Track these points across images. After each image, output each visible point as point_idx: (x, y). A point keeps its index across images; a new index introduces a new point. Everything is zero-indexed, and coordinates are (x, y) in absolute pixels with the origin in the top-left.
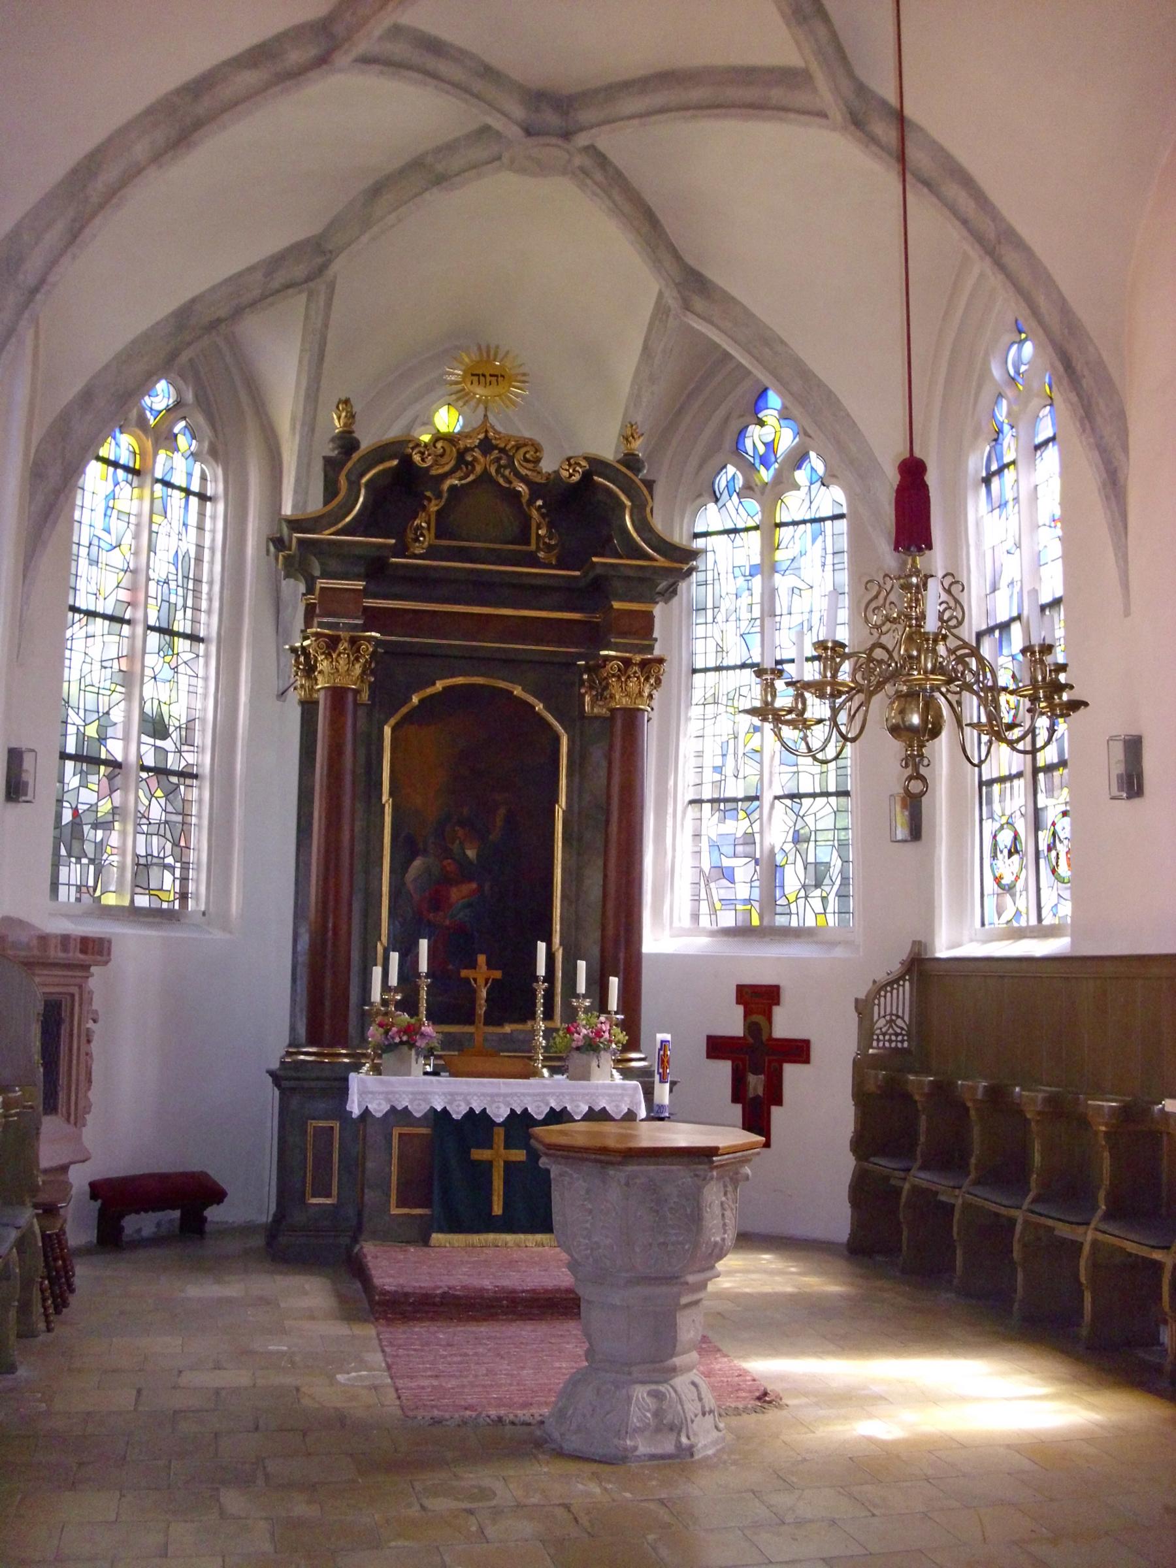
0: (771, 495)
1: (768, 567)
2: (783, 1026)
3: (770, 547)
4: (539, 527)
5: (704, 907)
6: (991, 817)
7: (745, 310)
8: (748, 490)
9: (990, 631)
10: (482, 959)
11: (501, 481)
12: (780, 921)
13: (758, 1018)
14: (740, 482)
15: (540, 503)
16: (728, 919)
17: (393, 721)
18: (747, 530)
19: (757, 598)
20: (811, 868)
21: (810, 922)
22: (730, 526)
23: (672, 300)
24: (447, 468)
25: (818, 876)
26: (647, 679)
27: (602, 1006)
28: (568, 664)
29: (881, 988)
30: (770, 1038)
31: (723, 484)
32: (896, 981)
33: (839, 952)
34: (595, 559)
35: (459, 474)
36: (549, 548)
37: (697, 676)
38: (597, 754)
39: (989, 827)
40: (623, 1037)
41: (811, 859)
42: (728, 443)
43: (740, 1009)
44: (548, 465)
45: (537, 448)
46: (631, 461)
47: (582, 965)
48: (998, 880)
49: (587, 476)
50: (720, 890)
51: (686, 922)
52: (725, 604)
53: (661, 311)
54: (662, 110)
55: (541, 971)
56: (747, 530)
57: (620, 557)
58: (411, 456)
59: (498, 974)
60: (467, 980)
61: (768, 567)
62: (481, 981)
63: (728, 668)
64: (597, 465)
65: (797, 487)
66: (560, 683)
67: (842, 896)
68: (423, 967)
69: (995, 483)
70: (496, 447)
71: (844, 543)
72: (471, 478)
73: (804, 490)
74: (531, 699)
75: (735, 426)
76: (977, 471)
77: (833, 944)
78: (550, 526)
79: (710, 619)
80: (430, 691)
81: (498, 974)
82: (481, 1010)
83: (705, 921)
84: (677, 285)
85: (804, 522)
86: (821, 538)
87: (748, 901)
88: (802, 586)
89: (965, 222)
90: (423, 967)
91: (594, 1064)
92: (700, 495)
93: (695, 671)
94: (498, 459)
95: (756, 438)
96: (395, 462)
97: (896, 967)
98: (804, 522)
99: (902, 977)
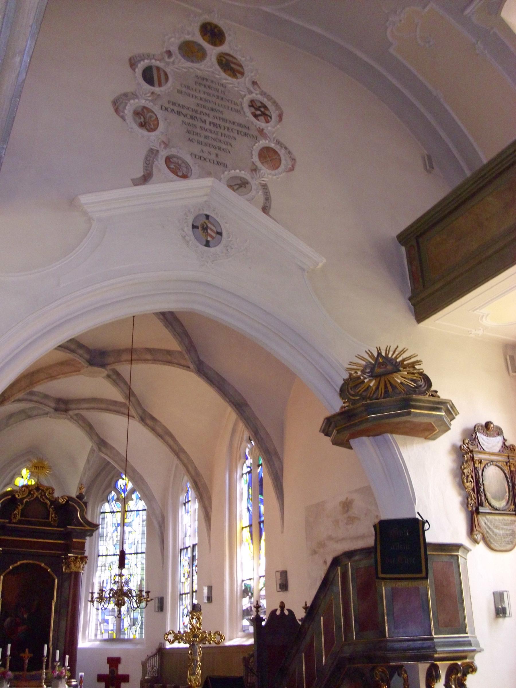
0: (125, 501)
1: (123, 524)
2: (122, 670)
3: (123, 518)
4: (52, 514)
5: (99, 632)
6: (182, 604)
7: (117, 451)
8: (118, 500)
9: (184, 549)
10: (27, 650)
11: (42, 500)
12: (122, 637)
13: (114, 669)
14: (116, 497)
15: (53, 506)
16: (106, 636)
17: (3, 574)
18: (117, 512)
19: (119, 534)
20: (132, 620)
21: (131, 637)
22: (112, 511)
23: (96, 449)
24: (25, 496)
25: (134, 622)
26: (82, 563)
27: (64, 665)
28: (59, 556)
29: (149, 658)
30: (117, 674)
31: (111, 497)
32: (154, 655)
33: (139, 647)
34: (68, 527)
35: (29, 497)
36: (55, 521)
37: (100, 558)
38: (66, 584)
39: (182, 608)
40: (69, 674)
41: (132, 617)
42: (112, 485)
43: (108, 665)
44: (56, 495)
45: (53, 490)
46: (80, 497)
47: (58, 652)
48: (184, 624)
49: (67, 501)
50: (103, 626)
51: (93, 637)
52: (109, 535)
53: (92, 451)
54: (93, 408)
55: (45, 654)
56: (117, 512)
57: (76, 526)
58: (15, 495)
59: (31, 655)
60: (22, 657)
61: (123, 524)
62: (26, 657)
63: (109, 555)
64: (70, 499)
65: (132, 500)
66: (56, 563)
67: (141, 628)
68: (9, 653)
69: (187, 505)
70: (41, 489)
71: (145, 517)
72: (32, 499)
73: (135, 501)
74: (46, 567)
75: (114, 480)
76: (182, 501)
77: (137, 644)
78: (55, 514)
79: (105, 539)
80: (15, 565)
81: (31, 655)
82: (26, 666)
83: (99, 637)
84: (97, 444)
85: (134, 511)
86: (138, 516)
87: (112, 630)
88: (132, 530)
89: (170, 447)
90: (9, 653)
91: (60, 683)
92: (103, 500)
93: (99, 556)
94: (41, 493)
95: (121, 483)
96: (10, 497)
97: (154, 651)
98: (134, 511)
99: (156, 654)
